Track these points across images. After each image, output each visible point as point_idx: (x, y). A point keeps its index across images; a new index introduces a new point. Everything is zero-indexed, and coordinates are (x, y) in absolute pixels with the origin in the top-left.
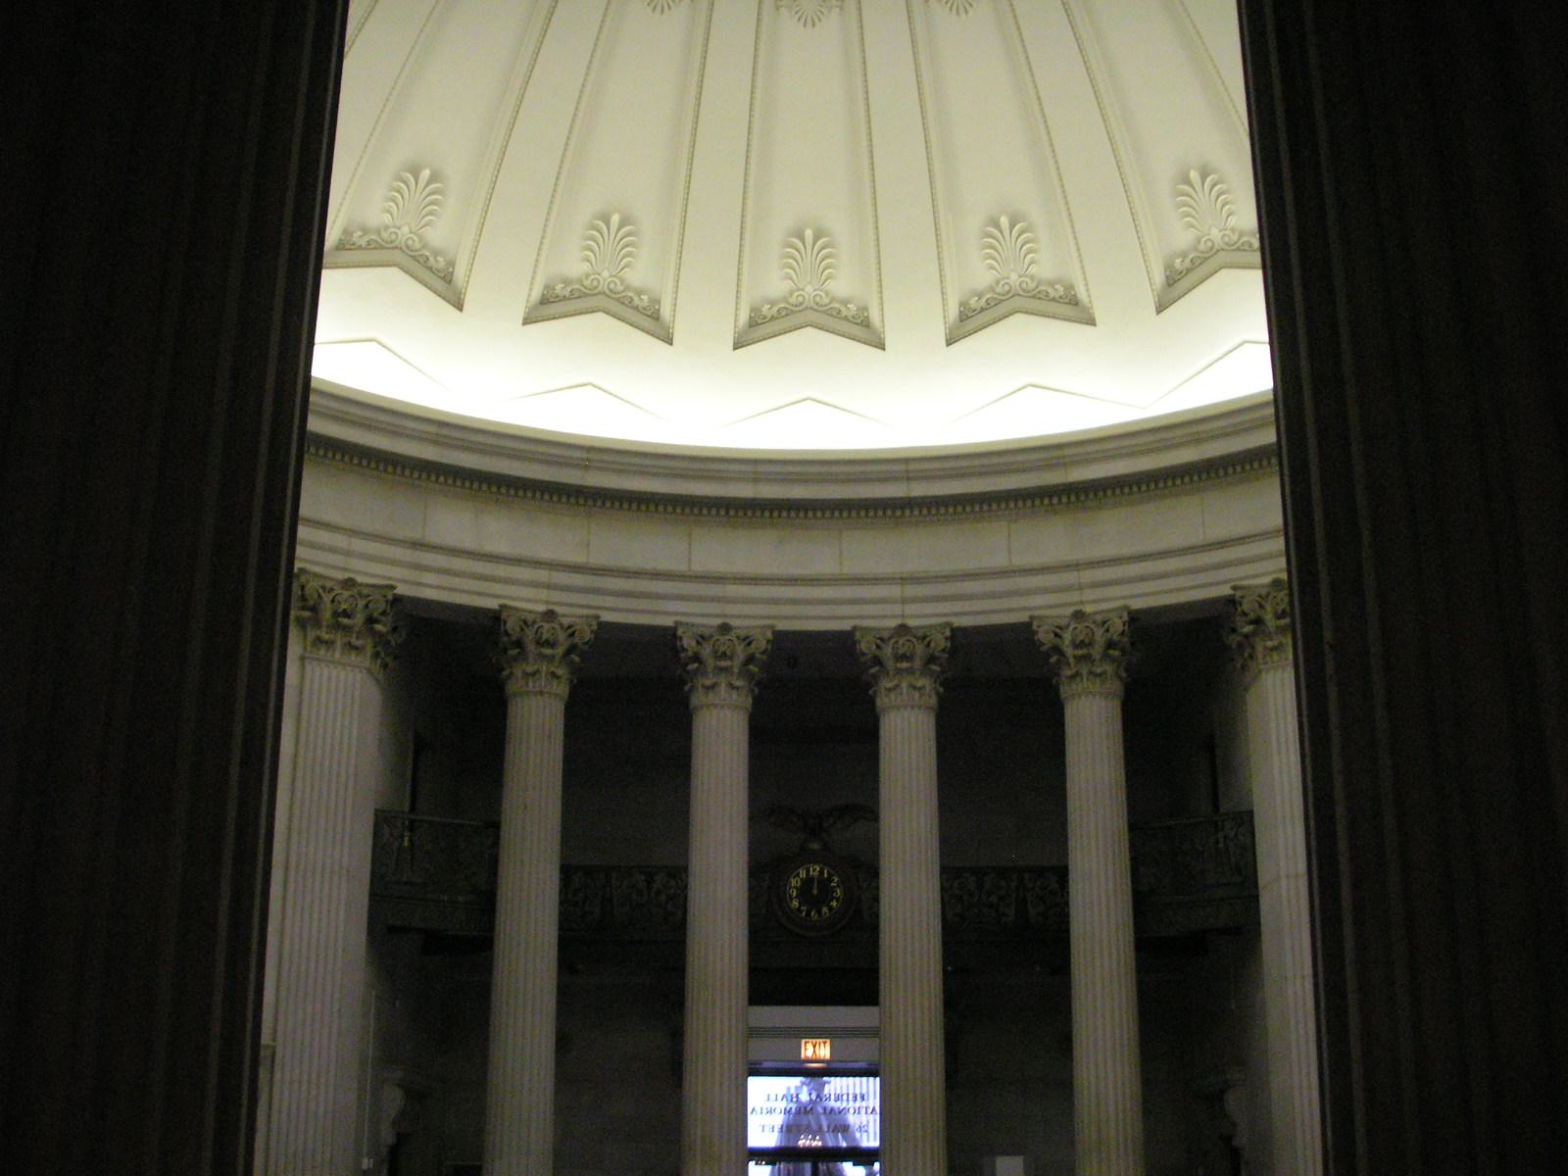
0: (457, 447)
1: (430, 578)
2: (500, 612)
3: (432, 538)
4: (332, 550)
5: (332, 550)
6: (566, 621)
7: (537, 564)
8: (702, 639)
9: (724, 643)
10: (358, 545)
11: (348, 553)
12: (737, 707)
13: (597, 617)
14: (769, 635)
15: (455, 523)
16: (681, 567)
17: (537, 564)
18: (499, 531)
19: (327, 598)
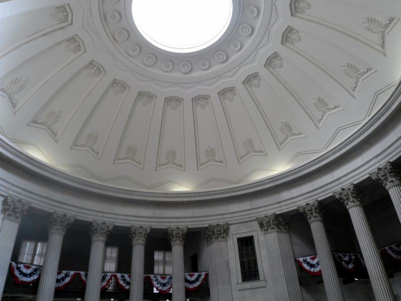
0: (277, 181)
1: (283, 208)
2: (297, 209)
3: (282, 200)
4: (263, 211)
5: (263, 211)
6: (312, 204)
7: (303, 195)
8: (340, 194)
9: (345, 192)
10: (267, 208)
11: (266, 210)
12: (355, 206)
13: (317, 200)
14: (353, 186)
15: (286, 195)
16: (333, 180)
17: (303, 195)
18: (295, 192)
19: (264, 221)
